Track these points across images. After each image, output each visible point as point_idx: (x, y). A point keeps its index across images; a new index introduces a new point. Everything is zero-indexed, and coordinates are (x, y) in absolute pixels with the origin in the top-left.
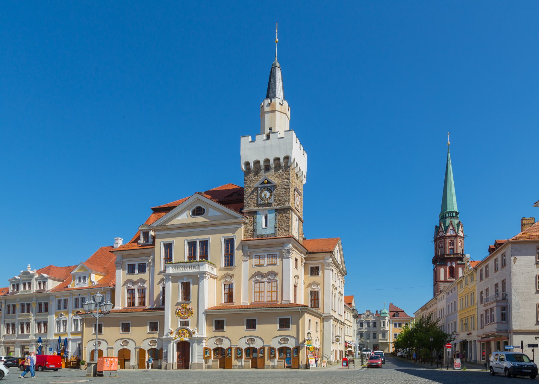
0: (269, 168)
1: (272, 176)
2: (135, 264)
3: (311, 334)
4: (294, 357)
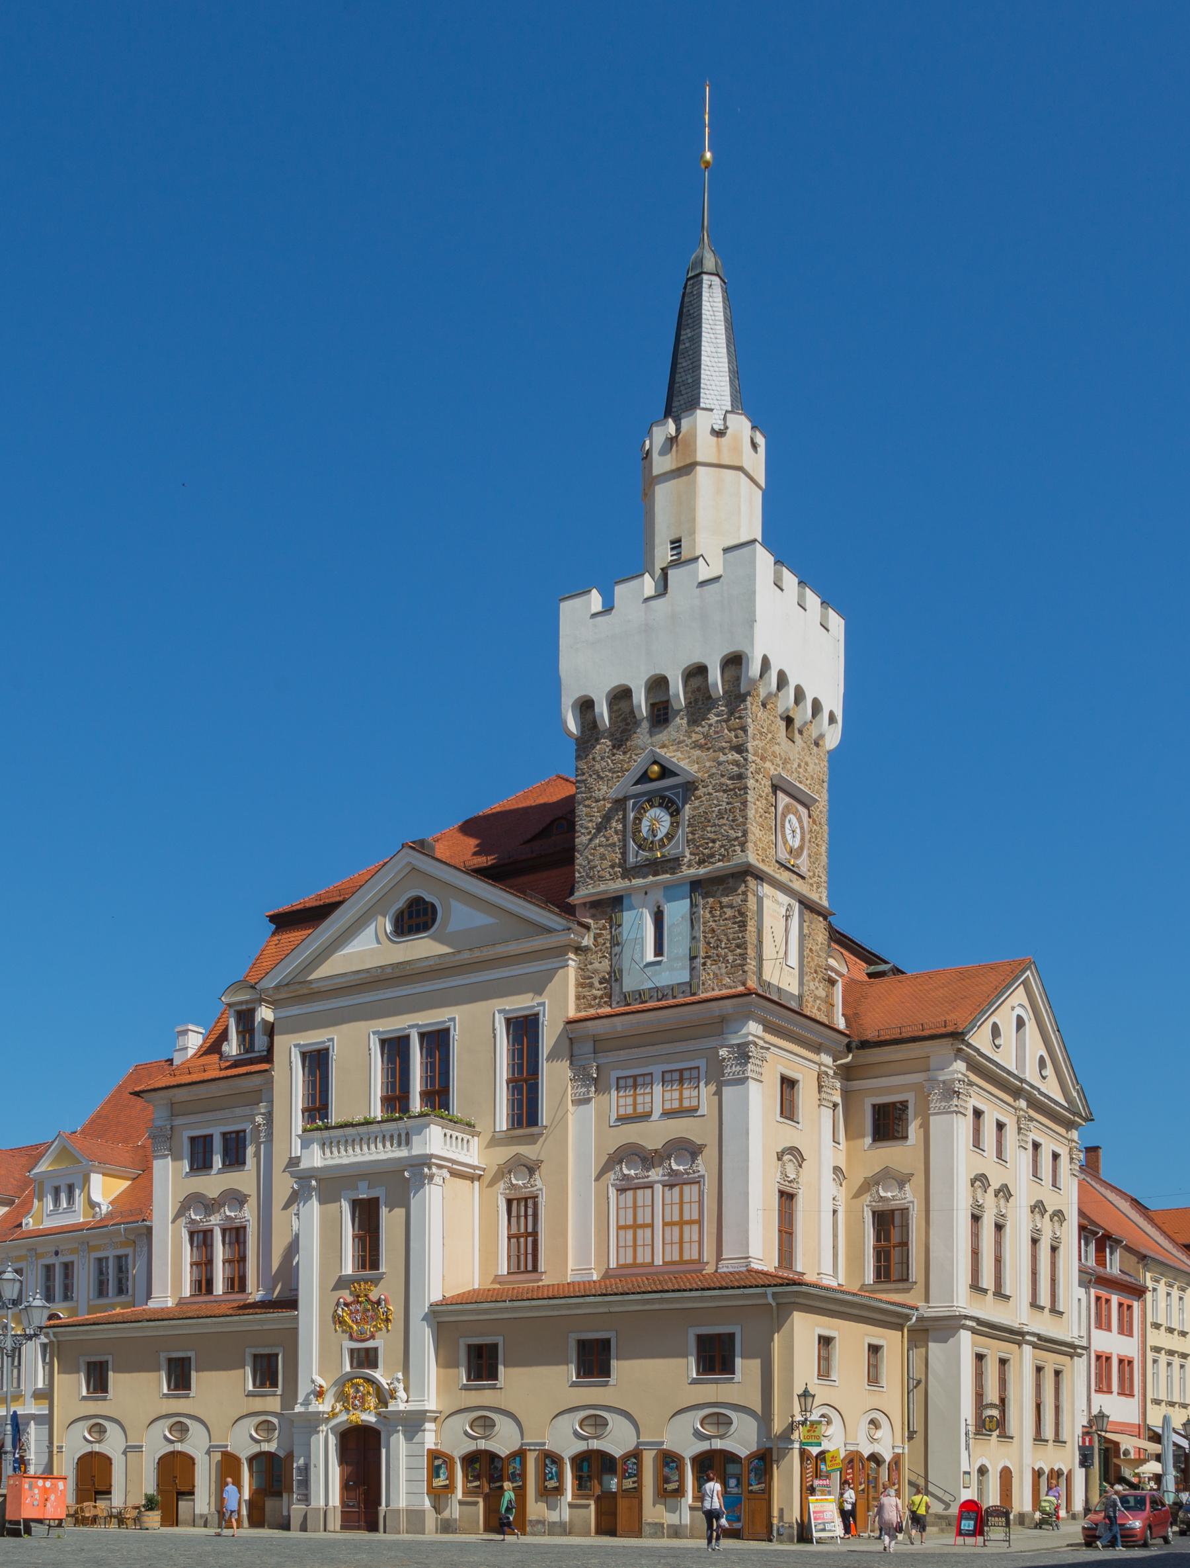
0: (667, 714)
2: (211, 1136)
3: (814, 1396)
4: (751, 1492)
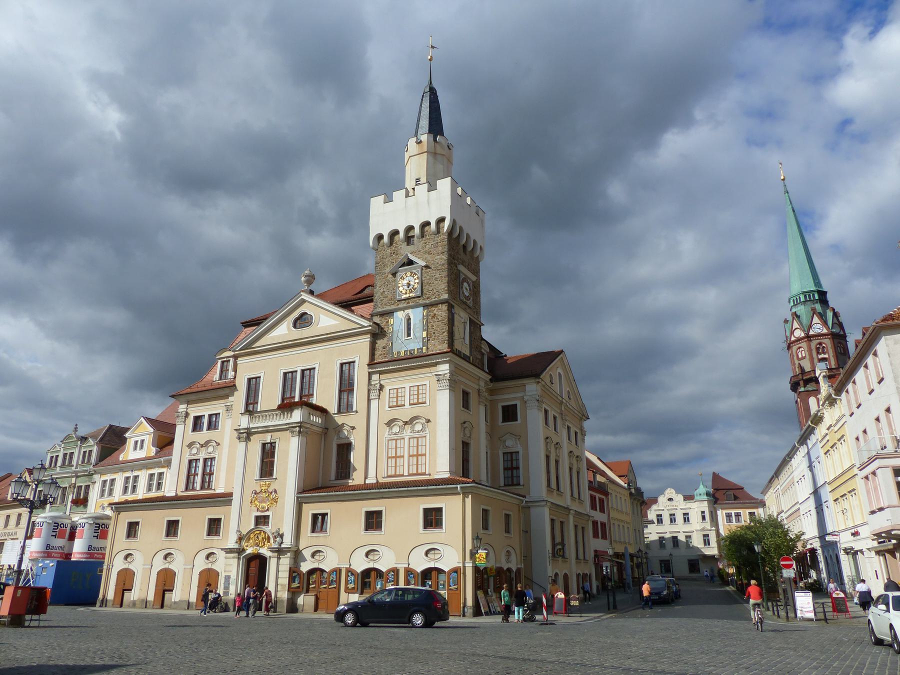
1: (419, 251)
3: (481, 539)
4: (451, 589)
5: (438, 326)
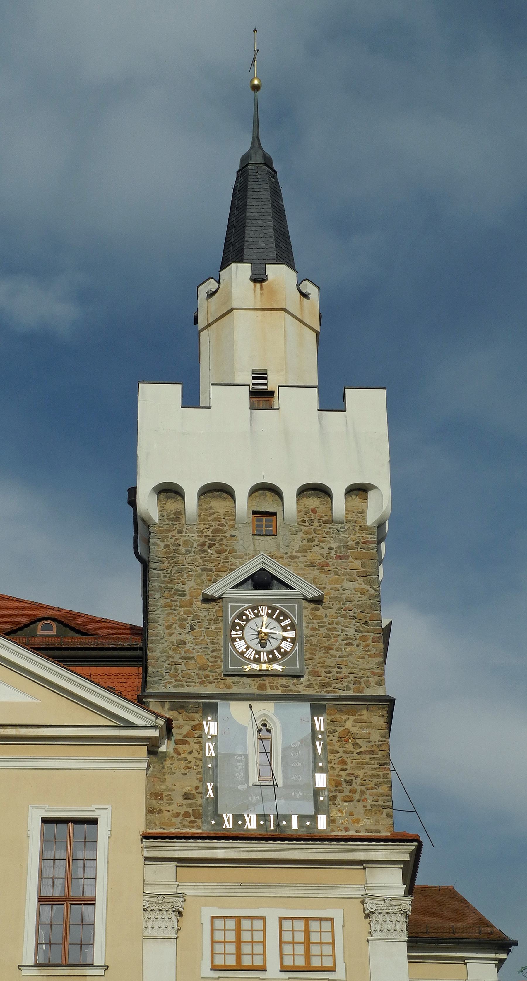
1: (292, 557)
5: (361, 765)
